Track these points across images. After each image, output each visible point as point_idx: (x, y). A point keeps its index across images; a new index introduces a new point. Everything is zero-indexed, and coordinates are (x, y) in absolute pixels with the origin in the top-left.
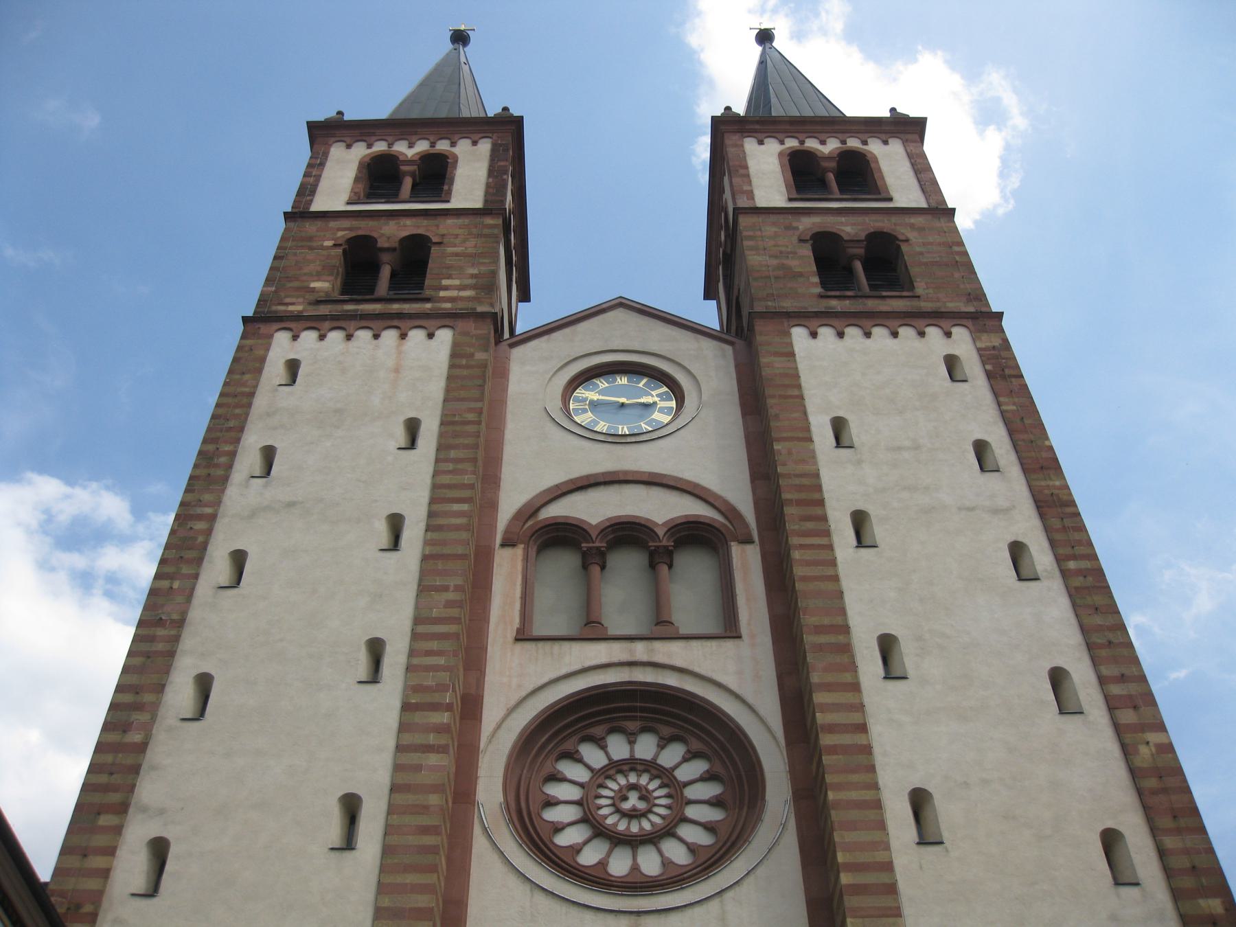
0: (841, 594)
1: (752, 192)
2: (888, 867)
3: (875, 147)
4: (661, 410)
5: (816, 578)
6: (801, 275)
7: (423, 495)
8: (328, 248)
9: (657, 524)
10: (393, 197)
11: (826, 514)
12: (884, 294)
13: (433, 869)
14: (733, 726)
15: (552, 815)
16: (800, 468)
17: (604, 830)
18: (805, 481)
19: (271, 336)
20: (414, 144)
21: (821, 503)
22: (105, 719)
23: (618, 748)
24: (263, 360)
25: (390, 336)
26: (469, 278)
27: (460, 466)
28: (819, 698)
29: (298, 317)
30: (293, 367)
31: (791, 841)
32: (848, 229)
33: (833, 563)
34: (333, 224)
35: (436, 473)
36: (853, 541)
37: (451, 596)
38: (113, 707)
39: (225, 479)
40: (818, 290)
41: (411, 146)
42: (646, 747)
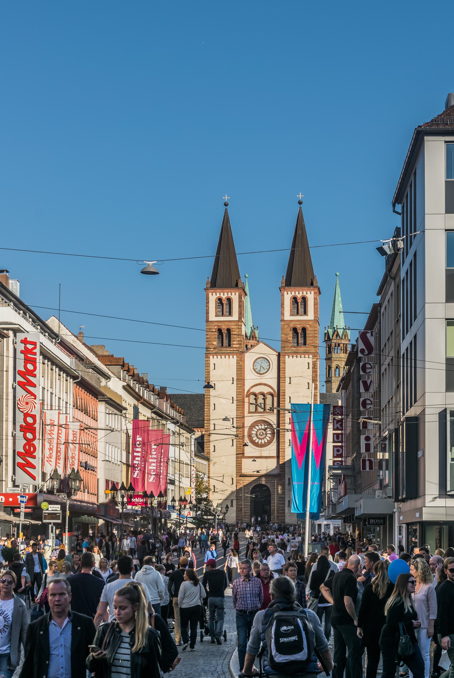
13: (241, 449)
16: (283, 389)
18: (283, 391)
19: (209, 358)
24: (209, 364)
27: (240, 388)
32: (298, 326)
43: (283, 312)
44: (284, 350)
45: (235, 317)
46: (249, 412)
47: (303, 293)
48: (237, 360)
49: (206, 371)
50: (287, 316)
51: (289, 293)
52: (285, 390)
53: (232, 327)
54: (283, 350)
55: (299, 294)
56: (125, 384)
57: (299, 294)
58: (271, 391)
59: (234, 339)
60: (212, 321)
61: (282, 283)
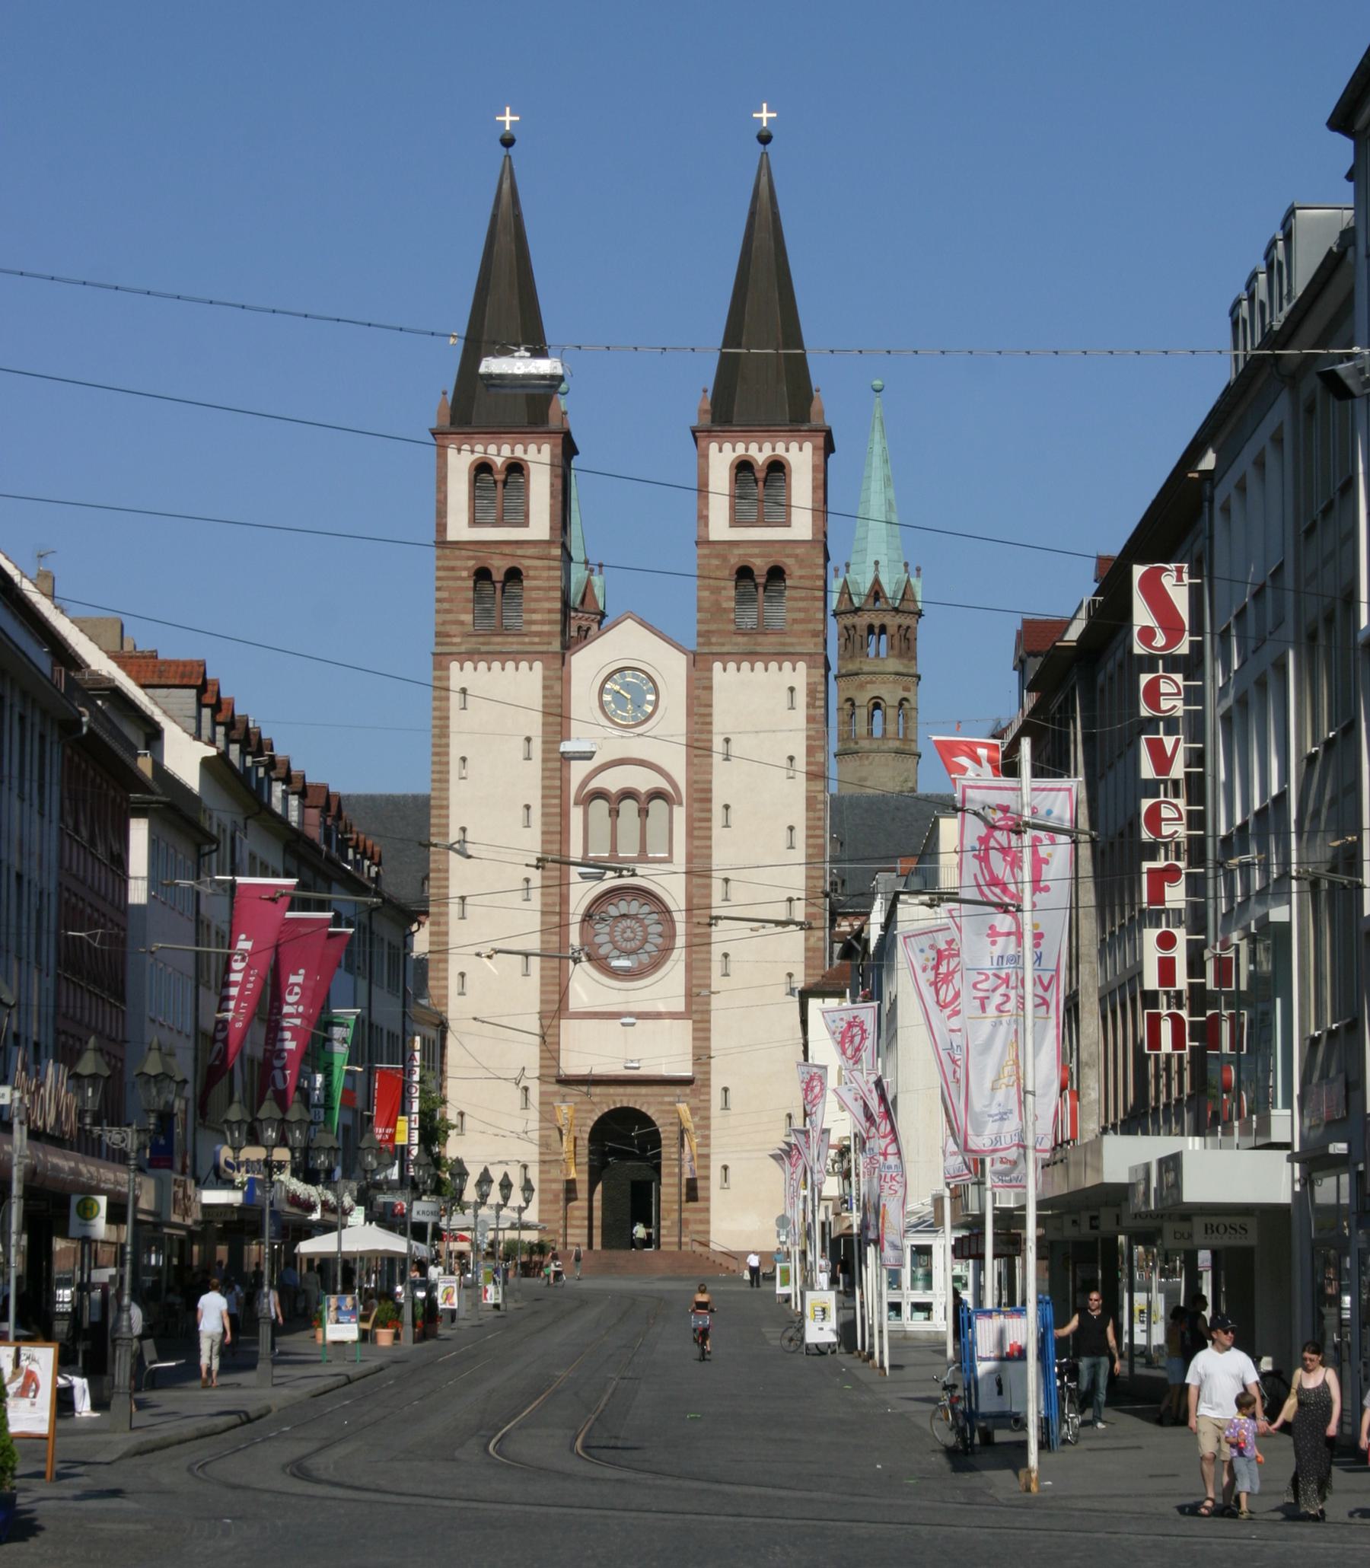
1: (706, 517)
6: (725, 610)
7: (538, 793)
18: (706, 786)
19: (448, 669)
25: (510, 665)
33: (710, 838)
39: (447, 781)
43: (705, 513)
44: (710, 644)
45: (539, 526)
47: (774, 449)
48: (545, 678)
49: (437, 714)
50: (720, 528)
51: (727, 446)
52: (710, 782)
53: (527, 562)
54: (703, 644)
55: (760, 450)
56: (212, 752)
57: (760, 450)
58: (662, 783)
59: (533, 605)
61: (702, 412)
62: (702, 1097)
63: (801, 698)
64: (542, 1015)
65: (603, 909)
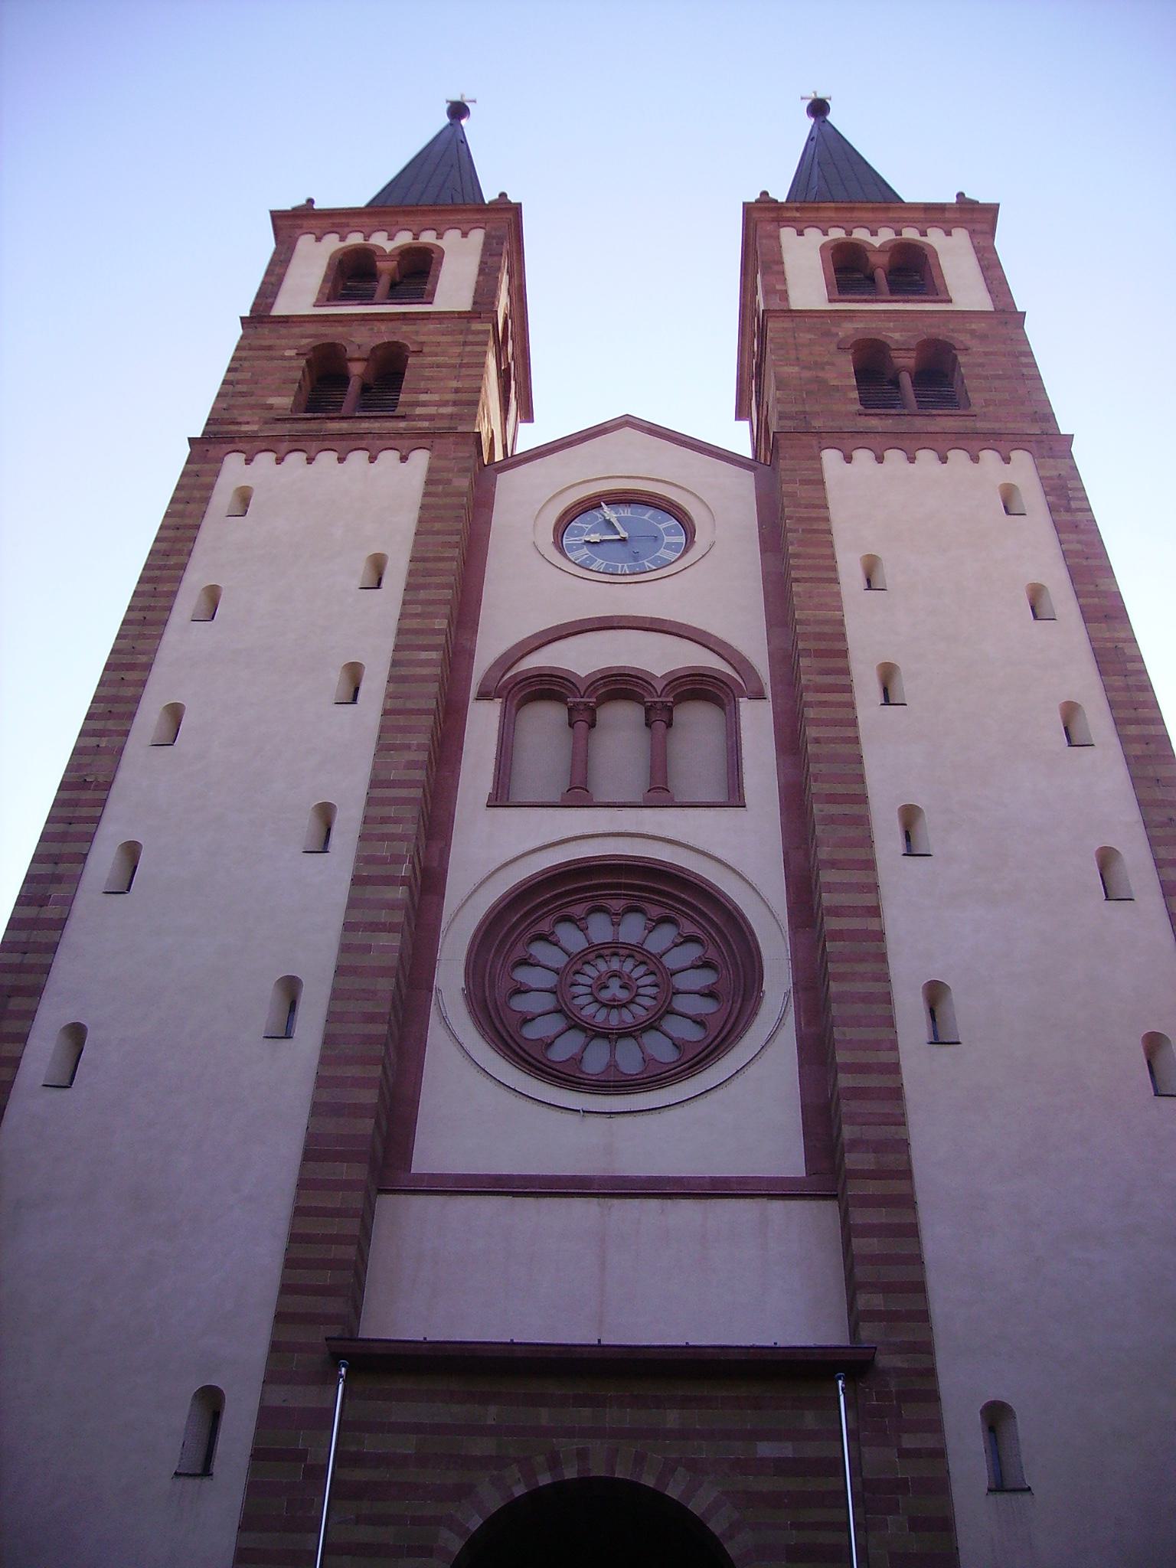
0: (859, 759)
1: (786, 291)
2: (895, 1068)
3: (935, 238)
4: (669, 546)
5: (833, 740)
6: (836, 388)
8: (290, 358)
9: (654, 677)
10: (367, 298)
11: (848, 668)
12: (934, 412)
14: (731, 908)
15: (520, 1003)
16: (822, 614)
17: (579, 1021)
18: (827, 629)
19: (221, 460)
20: (395, 235)
21: (844, 654)
22: (20, 892)
23: (600, 929)
25: (358, 459)
26: (452, 393)
27: (431, 609)
28: (827, 876)
29: (252, 437)
30: (244, 498)
31: (788, 1037)
32: (897, 336)
33: (853, 723)
34: (297, 330)
35: (403, 616)
36: (879, 698)
37: (412, 756)
38: (30, 879)
40: (858, 407)
41: (391, 238)
42: (632, 929)
46: (500, 798)
60: (286, 320)
62: (909, 1441)
63: (1033, 497)
64: (314, 1151)
65: (544, 927)
